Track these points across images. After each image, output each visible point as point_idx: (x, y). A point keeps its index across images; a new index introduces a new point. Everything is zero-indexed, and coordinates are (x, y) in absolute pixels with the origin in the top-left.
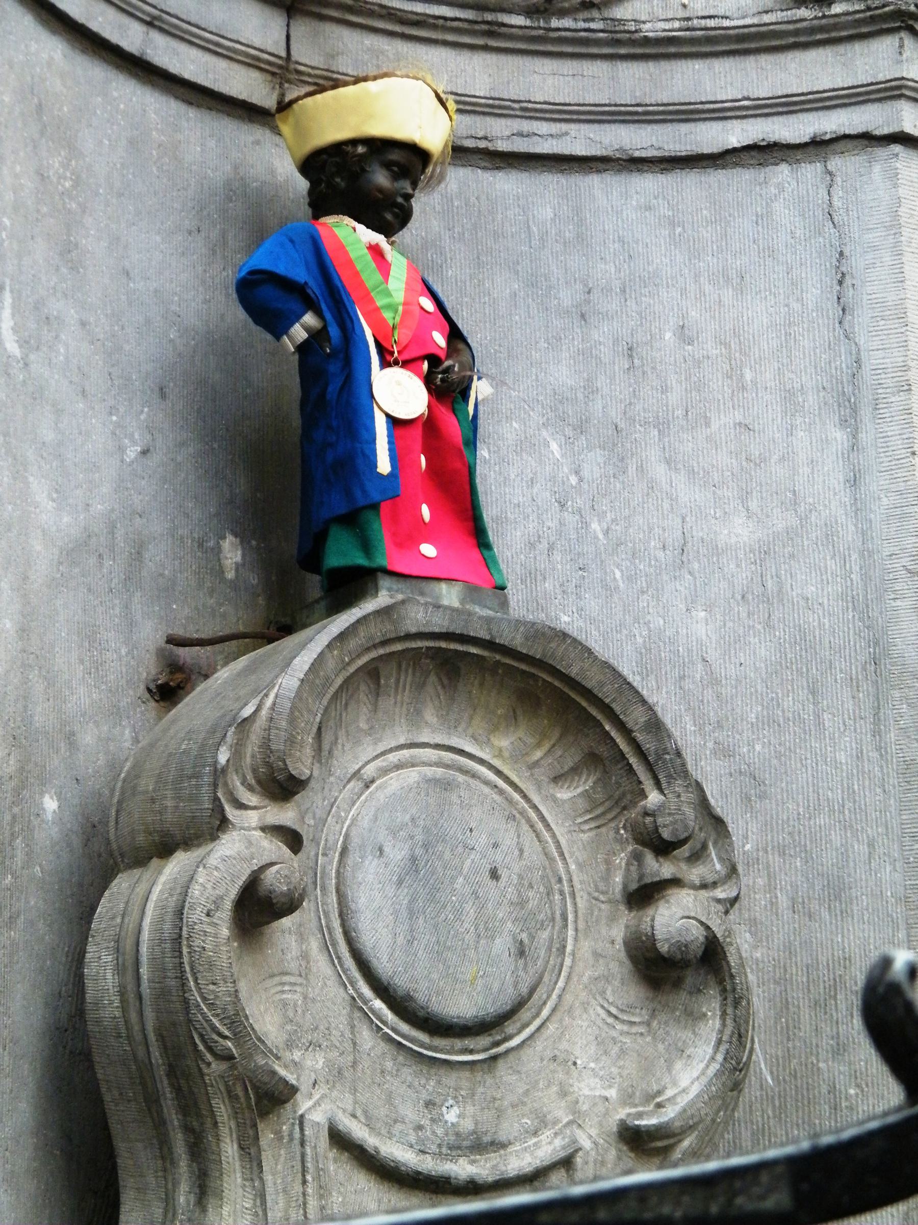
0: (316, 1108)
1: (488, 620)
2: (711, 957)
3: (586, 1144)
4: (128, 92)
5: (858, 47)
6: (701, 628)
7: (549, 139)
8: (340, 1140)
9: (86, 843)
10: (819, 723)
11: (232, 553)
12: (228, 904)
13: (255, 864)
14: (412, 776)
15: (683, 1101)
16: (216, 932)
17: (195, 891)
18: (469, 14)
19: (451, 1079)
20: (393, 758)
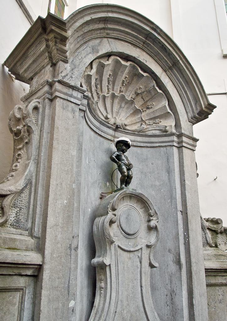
1: (135, 192)
2: (156, 228)
3: (143, 246)
4: (99, 137)
5: (170, 137)
7: (139, 144)
8: (119, 247)
9: (93, 214)
10: (165, 203)
11: (108, 184)
12: (109, 222)
13: (112, 218)
14: (127, 208)
15: (153, 242)
16: (107, 224)
17: (105, 221)
18: (133, 132)
19: (129, 240)
20: (125, 206)
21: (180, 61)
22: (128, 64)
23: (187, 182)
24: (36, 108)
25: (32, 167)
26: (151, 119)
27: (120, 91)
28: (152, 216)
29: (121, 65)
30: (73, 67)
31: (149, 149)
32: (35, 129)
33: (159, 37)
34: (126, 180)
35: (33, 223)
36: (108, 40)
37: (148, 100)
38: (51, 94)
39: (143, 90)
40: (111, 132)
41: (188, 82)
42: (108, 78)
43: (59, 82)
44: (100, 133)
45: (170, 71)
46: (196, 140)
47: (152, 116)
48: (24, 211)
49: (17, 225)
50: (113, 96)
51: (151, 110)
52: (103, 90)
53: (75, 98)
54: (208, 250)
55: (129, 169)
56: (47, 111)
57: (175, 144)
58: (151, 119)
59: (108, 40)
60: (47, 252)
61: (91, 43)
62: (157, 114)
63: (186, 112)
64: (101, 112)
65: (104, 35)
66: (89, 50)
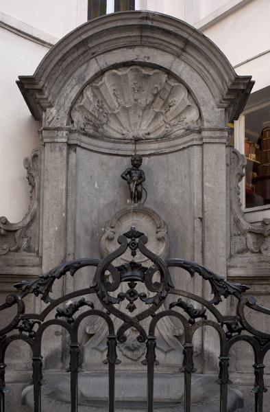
6: (177, 202)
11: (128, 201)
21: (191, 39)
22: (127, 71)
23: (206, 184)
26: (175, 118)
27: (136, 100)
28: (159, 228)
29: (119, 76)
30: (58, 108)
31: (177, 153)
33: (155, 24)
36: (97, 60)
37: (168, 97)
39: (159, 89)
40: (131, 147)
42: (114, 94)
43: (44, 129)
44: (115, 152)
45: (184, 53)
47: (176, 114)
51: (174, 107)
52: (113, 107)
53: (61, 137)
54: (247, 257)
56: (43, 156)
57: (195, 142)
58: (175, 118)
59: (97, 60)
60: (43, 267)
61: (76, 74)
63: (212, 97)
64: (115, 131)
65: (90, 56)
66: (74, 82)
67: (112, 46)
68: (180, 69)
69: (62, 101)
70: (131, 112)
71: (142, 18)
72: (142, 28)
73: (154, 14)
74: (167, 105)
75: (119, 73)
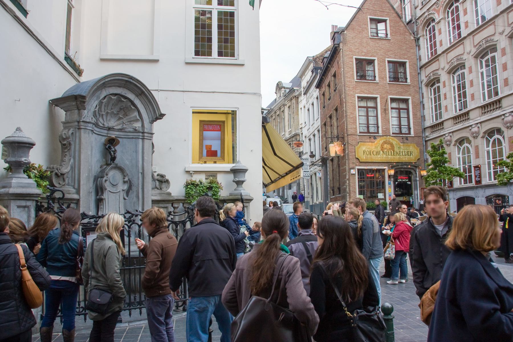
0: (108, 189)
21: (146, 92)
24: (72, 133)
25: (72, 160)
32: (72, 143)
34: (113, 159)
35: (75, 183)
38: (79, 126)
40: (106, 132)
41: (150, 102)
43: (83, 121)
46: (152, 134)
47: (129, 120)
48: (70, 179)
49: (68, 185)
50: (107, 113)
51: (129, 117)
55: (114, 154)
56: (77, 134)
57: (140, 137)
62: (132, 119)
66: (95, 98)
67: (113, 85)
68: (137, 102)
69: (90, 108)
70: (109, 115)
71: (129, 78)
72: (127, 81)
73: (134, 78)
74: (126, 115)
75: (113, 98)
